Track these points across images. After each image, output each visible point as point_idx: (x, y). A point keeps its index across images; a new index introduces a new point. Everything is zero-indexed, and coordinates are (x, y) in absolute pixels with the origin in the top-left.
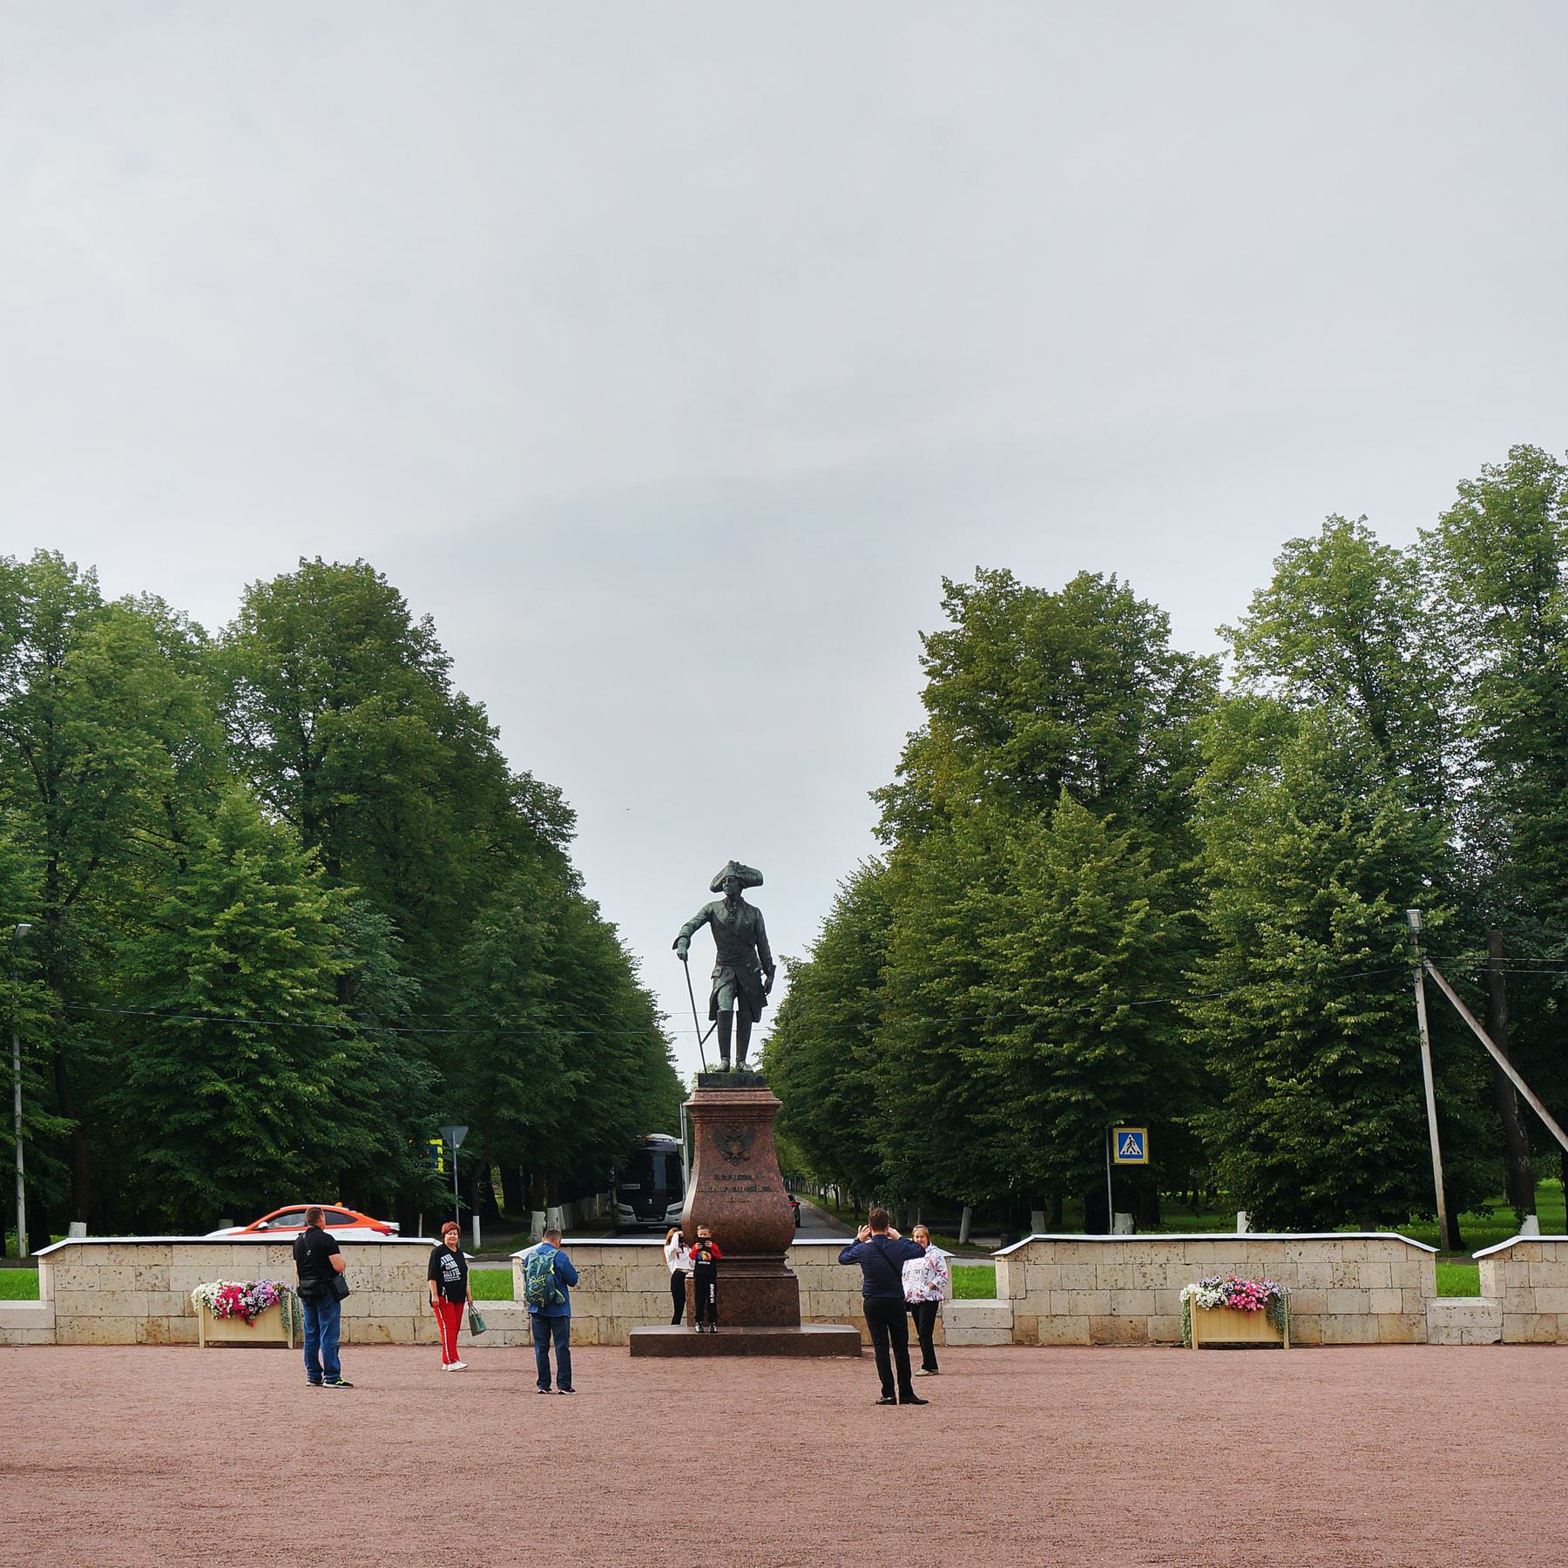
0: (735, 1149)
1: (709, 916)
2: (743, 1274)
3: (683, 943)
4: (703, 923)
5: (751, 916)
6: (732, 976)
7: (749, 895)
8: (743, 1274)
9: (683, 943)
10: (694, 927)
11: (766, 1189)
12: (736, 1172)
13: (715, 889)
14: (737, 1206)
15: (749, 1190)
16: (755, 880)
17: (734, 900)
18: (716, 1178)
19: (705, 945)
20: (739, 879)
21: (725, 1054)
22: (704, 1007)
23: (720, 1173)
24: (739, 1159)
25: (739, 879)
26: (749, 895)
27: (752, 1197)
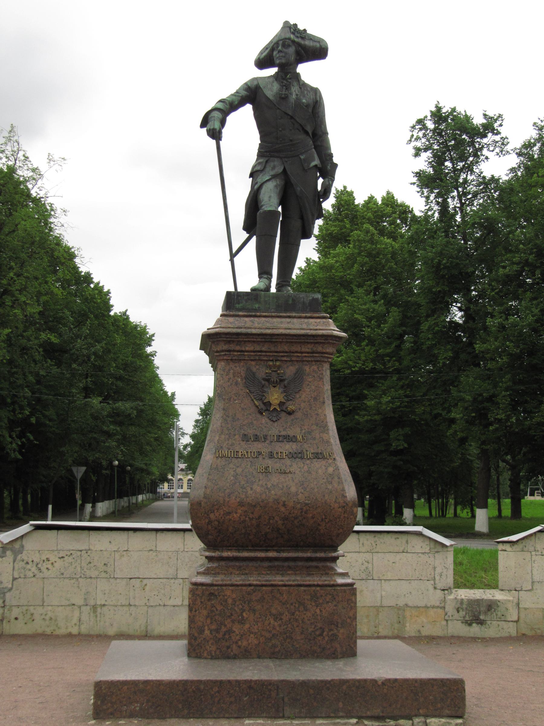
0: (275, 396)
1: (251, 94)
2: (278, 579)
3: (213, 123)
4: (241, 103)
5: (311, 96)
6: (279, 169)
7: (308, 72)
8: (278, 579)
9: (213, 123)
10: (229, 107)
11: (318, 456)
12: (275, 430)
13: (261, 63)
14: (275, 479)
15: (293, 456)
16: (317, 51)
17: (288, 76)
18: (245, 438)
19: (244, 131)
20: (294, 48)
21: (264, 271)
22: (238, 215)
23: (250, 432)
24: (283, 411)
25: (294, 48)
26: (308, 72)
27: (296, 466)
